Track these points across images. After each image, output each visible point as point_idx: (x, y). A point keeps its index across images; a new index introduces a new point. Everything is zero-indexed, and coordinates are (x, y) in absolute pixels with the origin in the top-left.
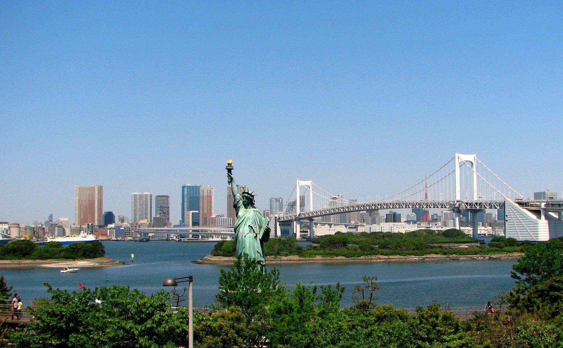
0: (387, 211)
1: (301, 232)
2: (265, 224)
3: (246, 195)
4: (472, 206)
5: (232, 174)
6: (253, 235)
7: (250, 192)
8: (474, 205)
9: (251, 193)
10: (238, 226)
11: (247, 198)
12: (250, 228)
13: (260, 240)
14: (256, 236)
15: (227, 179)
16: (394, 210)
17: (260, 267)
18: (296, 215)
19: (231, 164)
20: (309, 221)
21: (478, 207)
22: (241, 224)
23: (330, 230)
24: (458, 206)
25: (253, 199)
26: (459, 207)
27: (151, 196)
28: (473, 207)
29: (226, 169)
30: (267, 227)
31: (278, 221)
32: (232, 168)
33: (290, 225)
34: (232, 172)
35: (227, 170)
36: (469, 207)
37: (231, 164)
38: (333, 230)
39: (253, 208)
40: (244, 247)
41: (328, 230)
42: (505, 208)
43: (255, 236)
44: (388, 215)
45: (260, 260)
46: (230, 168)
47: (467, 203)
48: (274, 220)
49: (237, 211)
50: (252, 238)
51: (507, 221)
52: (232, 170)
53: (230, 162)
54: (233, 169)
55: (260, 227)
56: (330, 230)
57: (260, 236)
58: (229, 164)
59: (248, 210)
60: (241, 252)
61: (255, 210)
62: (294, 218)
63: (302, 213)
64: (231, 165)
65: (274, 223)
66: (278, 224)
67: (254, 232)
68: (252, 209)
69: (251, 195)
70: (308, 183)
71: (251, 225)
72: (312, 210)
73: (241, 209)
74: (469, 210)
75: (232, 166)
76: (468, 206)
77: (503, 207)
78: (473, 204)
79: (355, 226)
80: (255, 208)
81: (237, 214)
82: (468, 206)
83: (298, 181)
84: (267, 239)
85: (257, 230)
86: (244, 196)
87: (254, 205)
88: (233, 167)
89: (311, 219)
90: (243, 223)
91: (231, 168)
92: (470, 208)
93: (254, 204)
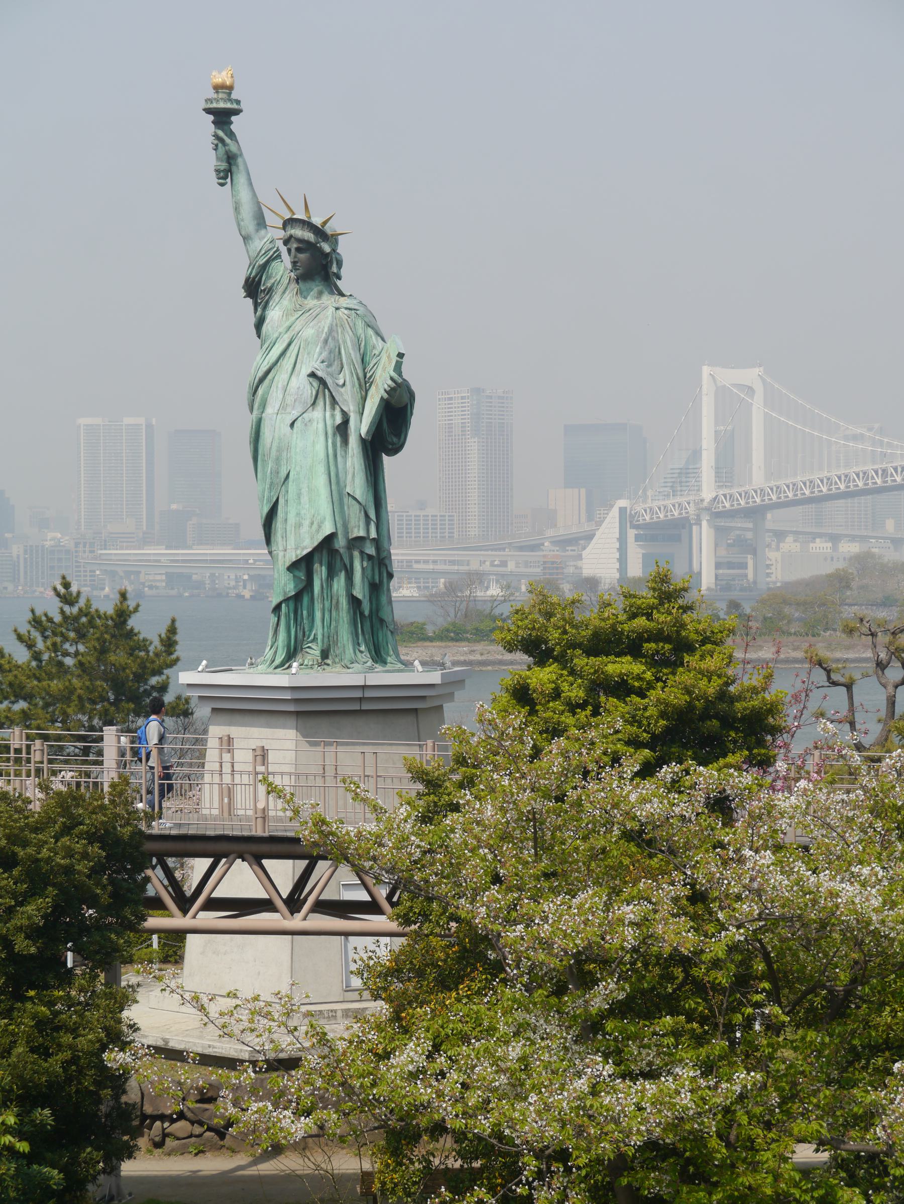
1: (718, 566)
2: (384, 369)
3: (298, 232)
5: (232, 135)
6: (328, 414)
7: (317, 221)
9: (325, 223)
10: (262, 380)
11: (304, 246)
12: (316, 384)
13: (363, 441)
14: (346, 422)
15: (211, 160)
17: (363, 569)
18: (702, 500)
19: (231, 88)
20: (750, 525)
22: (276, 368)
23: (832, 559)
25: (334, 250)
27: (149, 426)
29: (208, 111)
30: (392, 379)
31: (631, 522)
32: (235, 106)
34: (232, 127)
35: (211, 118)
37: (231, 88)
39: (332, 293)
40: (286, 473)
41: (826, 559)
43: (339, 420)
45: (362, 533)
46: (222, 105)
48: (617, 520)
49: (259, 309)
50: (326, 434)
52: (233, 118)
53: (222, 77)
54: (237, 112)
55: (365, 384)
56: (832, 559)
57: (361, 426)
58: (217, 88)
59: (311, 302)
60: (274, 499)
61: (343, 302)
62: (691, 512)
63: (722, 492)
64: (230, 94)
65: (617, 530)
66: (631, 533)
67: (334, 402)
68: (329, 300)
69: (319, 232)
70: (751, 376)
71: (319, 374)
72: (758, 478)
73: (276, 297)
75: (234, 96)
80: (342, 295)
81: (259, 324)
83: (706, 370)
84: (399, 439)
85: (348, 398)
86: (291, 236)
87: (339, 283)
88: (238, 102)
89: (755, 513)
90: (287, 363)
91: (229, 105)
93: (339, 278)
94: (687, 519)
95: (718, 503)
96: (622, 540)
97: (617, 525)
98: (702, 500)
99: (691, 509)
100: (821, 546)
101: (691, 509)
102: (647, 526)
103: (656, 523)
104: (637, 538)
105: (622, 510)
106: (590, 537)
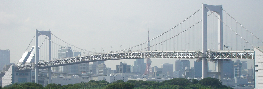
0: (118, 62)
4: (220, 56)
8: (222, 54)
16: (124, 61)
21: (226, 58)
23: (65, 80)
24: (205, 56)
26: (206, 57)
28: (221, 57)
33: (28, 75)
36: (216, 58)
38: (68, 80)
42: (254, 58)
44: (119, 66)
47: (214, 54)
48: (12, 69)
51: (257, 70)
65: (12, 72)
66: (15, 73)
74: (216, 60)
76: (215, 56)
77: (252, 57)
78: (220, 54)
79: (88, 76)
82: (215, 56)
89: (49, 68)
92: (218, 58)
94: (31, 69)
95: (39, 65)
96: (13, 75)
97: (12, 71)
98: (35, 64)
99: (32, 67)
100: (62, 76)
101: (32, 67)
102: (20, 71)
103: (23, 70)
104: (17, 74)
105: (13, 67)
106: (3, 74)
